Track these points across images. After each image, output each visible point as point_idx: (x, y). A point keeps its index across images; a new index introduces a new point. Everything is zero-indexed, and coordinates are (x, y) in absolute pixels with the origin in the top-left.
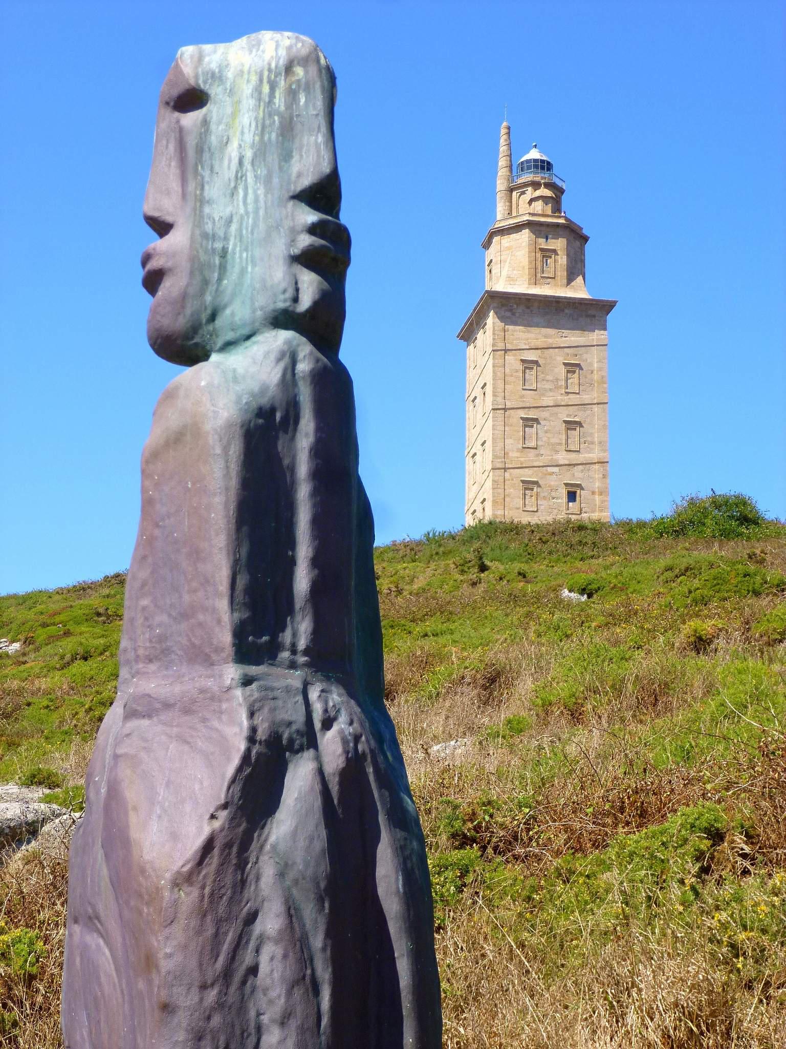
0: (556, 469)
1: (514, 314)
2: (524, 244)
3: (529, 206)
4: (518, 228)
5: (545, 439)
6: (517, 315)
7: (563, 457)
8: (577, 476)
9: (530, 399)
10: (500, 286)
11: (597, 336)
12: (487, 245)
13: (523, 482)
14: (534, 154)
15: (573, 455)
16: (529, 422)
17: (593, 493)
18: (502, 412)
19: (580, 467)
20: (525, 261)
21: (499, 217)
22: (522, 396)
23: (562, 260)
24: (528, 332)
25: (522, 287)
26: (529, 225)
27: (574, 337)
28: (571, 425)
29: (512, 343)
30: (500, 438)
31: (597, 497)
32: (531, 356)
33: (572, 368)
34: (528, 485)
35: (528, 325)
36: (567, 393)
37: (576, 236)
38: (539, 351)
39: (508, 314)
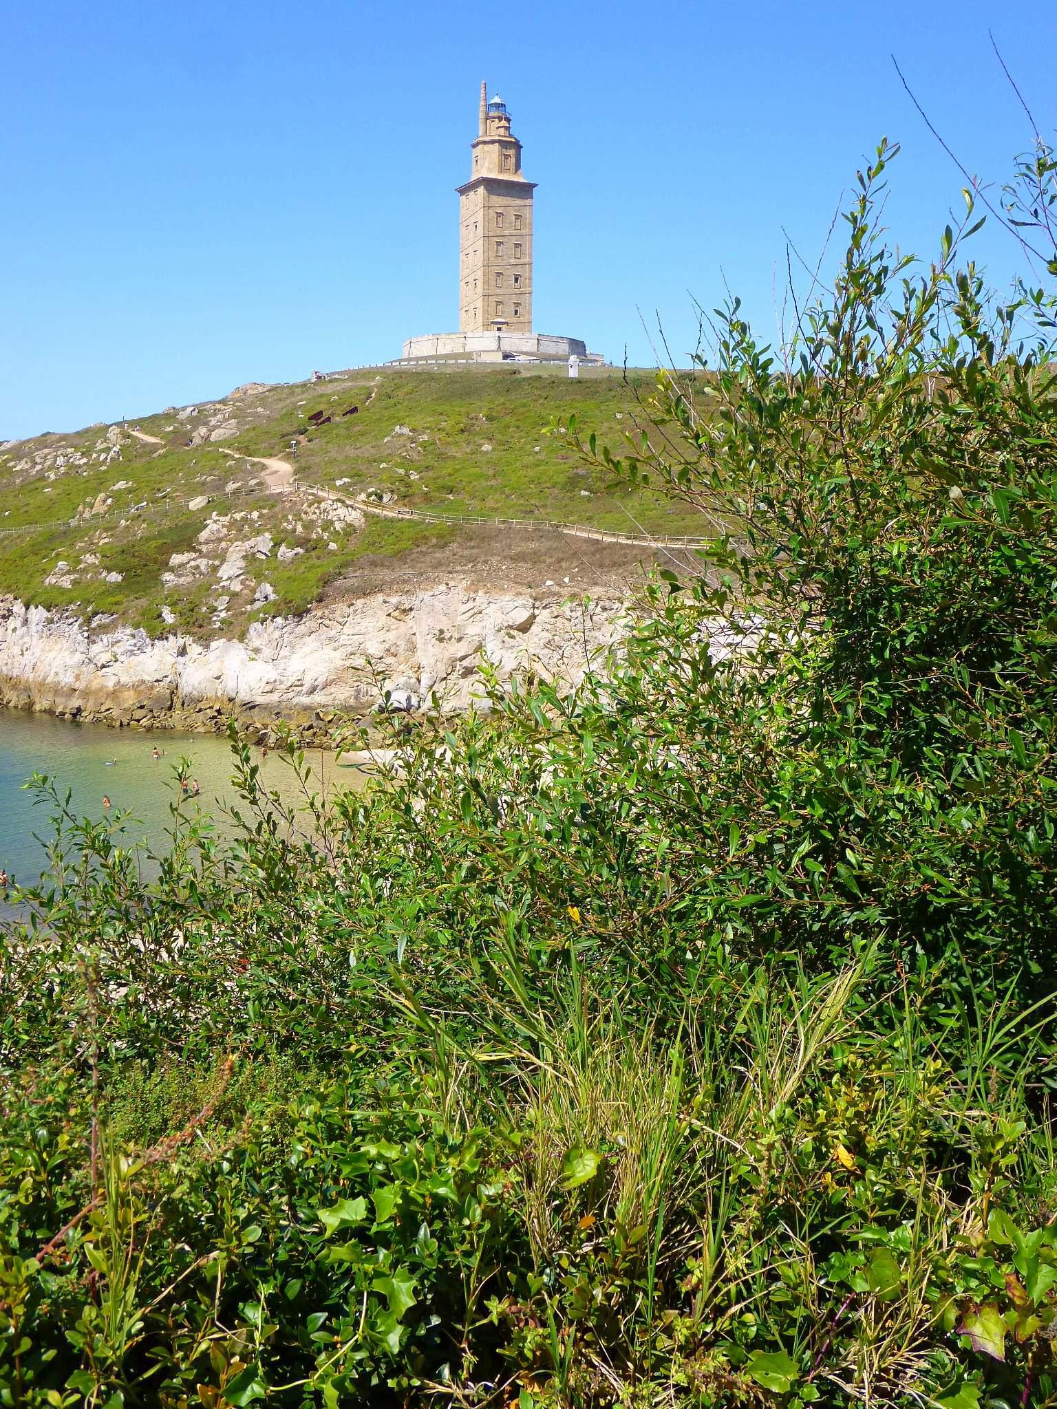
3: (496, 130)
4: (493, 142)
7: (513, 261)
8: (518, 271)
9: (499, 232)
10: (485, 174)
11: (528, 202)
12: (474, 146)
14: (497, 100)
16: (499, 243)
21: (481, 133)
23: (513, 160)
25: (494, 175)
26: (499, 142)
27: (519, 202)
28: (517, 245)
30: (486, 251)
33: (518, 217)
34: (499, 274)
37: (517, 146)
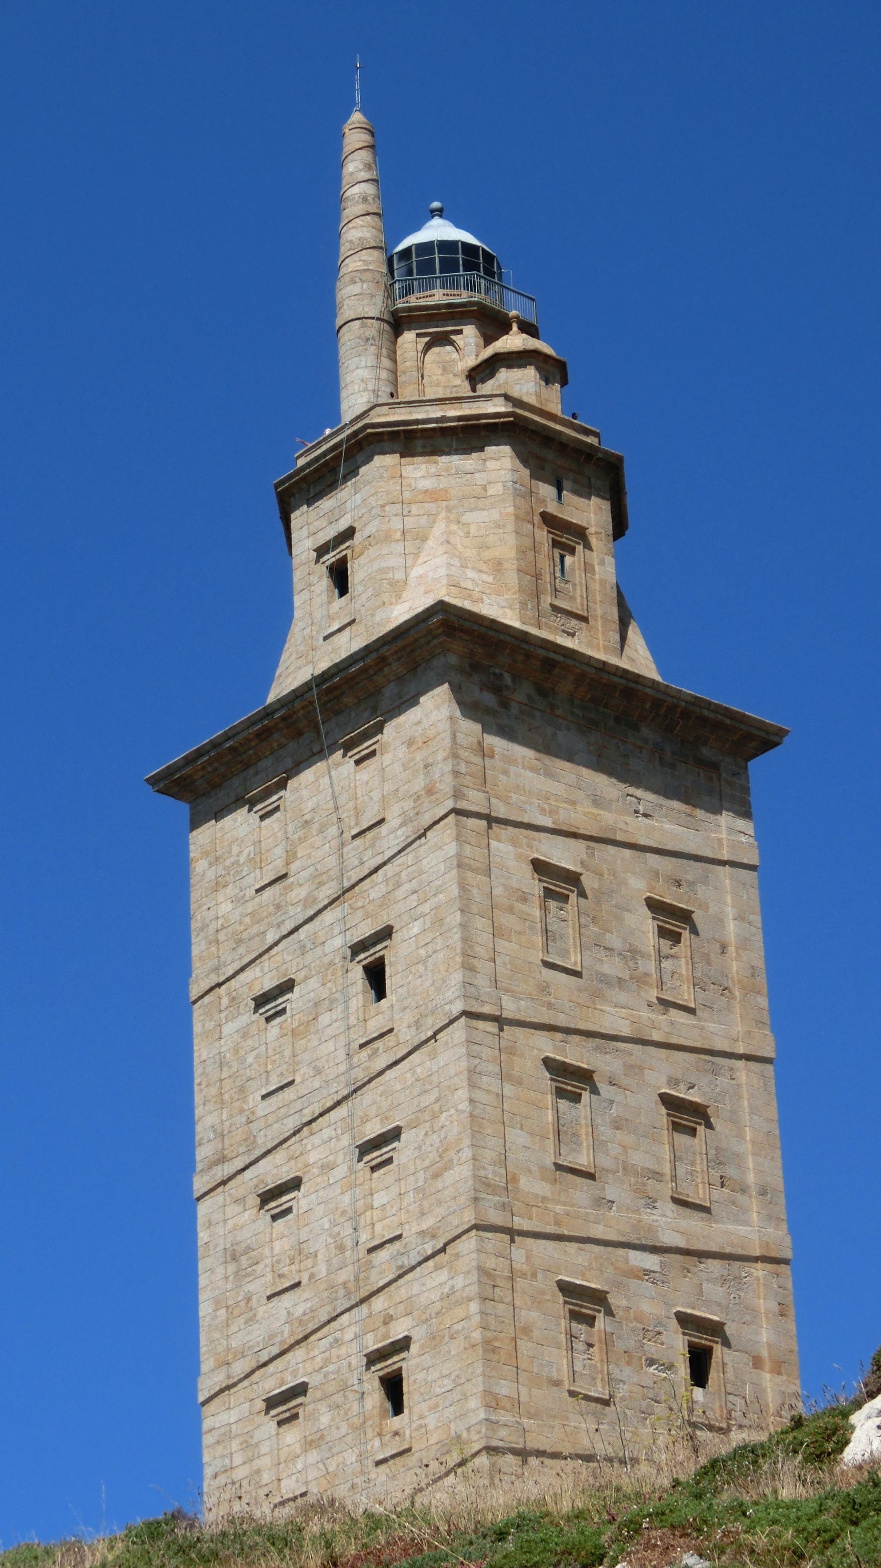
0: (651, 1261)
1: (505, 704)
2: (496, 490)
4: (470, 436)
5: (615, 1150)
6: (514, 709)
8: (707, 1293)
9: (565, 1000)
13: (565, 1288)
15: (693, 1222)
17: (757, 1363)
18: (491, 1027)
19: (715, 1266)
20: (506, 547)
22: (544, 988)
24: (549, 774)
26: (517, 431)
29: (506, 801)
31: (767, 1378)
32: (563, 855)
35: (547, 748)
36: (665, 1004)
38: (581, 845)
39: (489, 699)
